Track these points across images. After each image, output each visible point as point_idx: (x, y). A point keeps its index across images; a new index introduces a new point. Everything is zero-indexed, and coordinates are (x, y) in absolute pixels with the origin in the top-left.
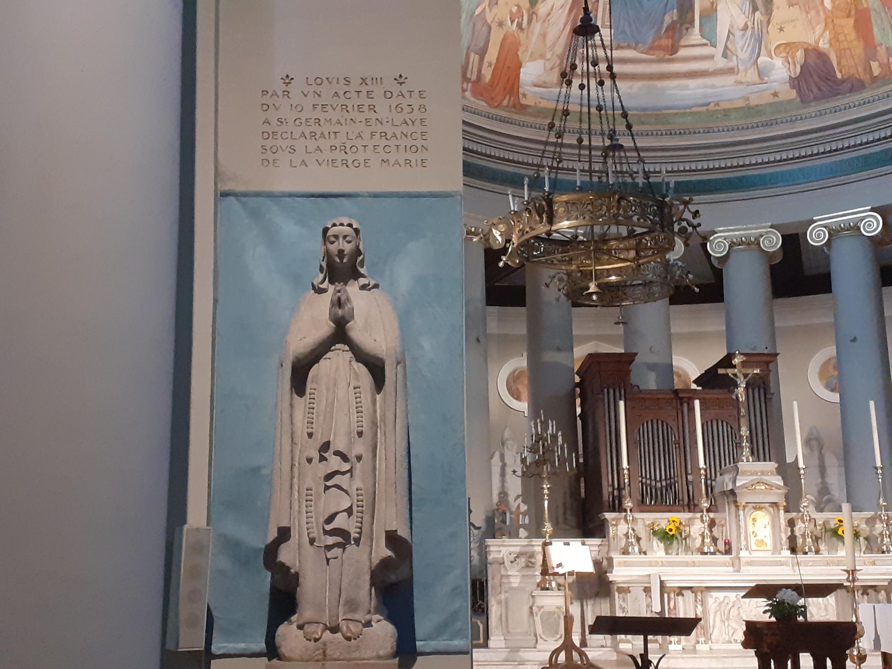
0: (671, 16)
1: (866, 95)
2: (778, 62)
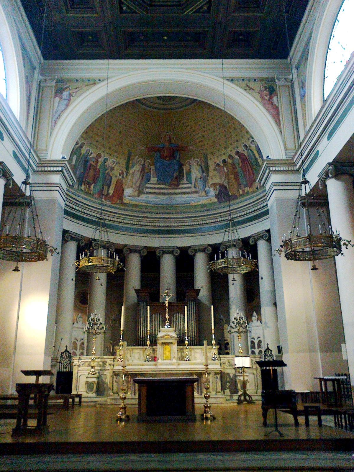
0: (176, 174)
1: (238, 201)
2: (211, 189)
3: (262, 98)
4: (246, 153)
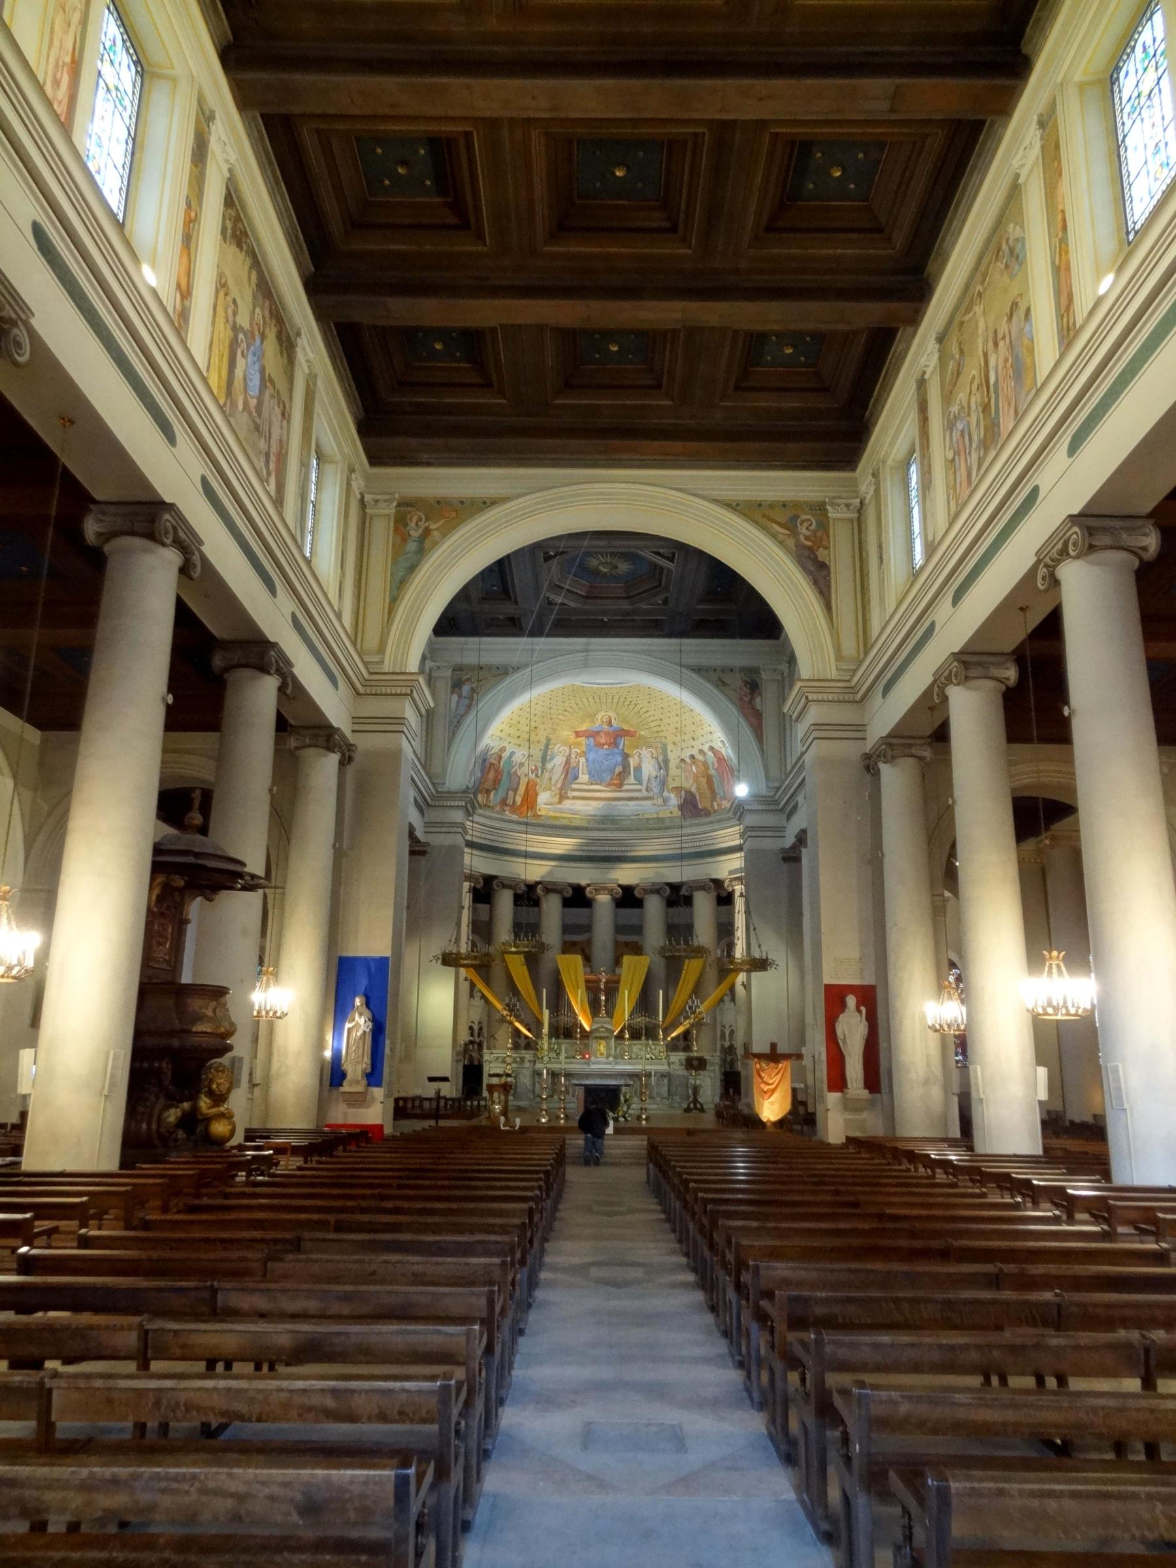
0: (619, 769)
2: (673, 796)
3: (741, 699)
4: (723, 751)
